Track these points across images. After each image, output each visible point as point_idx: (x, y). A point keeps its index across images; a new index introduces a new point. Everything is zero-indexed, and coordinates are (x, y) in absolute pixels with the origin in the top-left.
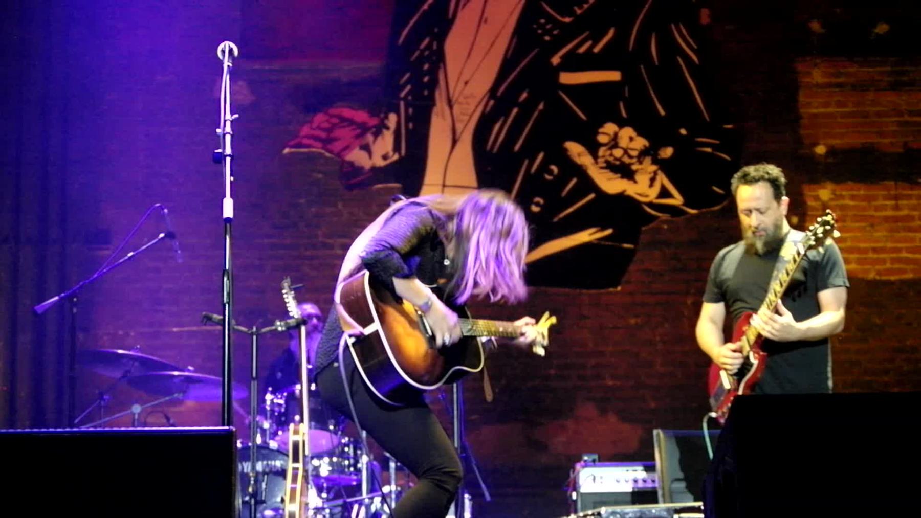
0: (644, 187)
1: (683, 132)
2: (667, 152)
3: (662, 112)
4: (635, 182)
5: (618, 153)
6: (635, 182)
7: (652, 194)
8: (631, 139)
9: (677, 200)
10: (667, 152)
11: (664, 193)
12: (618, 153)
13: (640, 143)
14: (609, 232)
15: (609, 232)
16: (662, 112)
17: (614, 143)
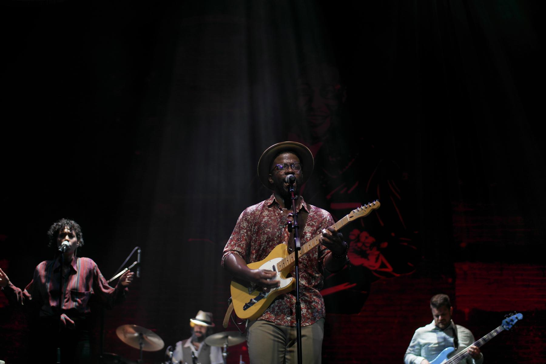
0: (372, 263)
1: (393, 234)
2: (385, 245)
3: (382, 224)
4: (368, 260)
5: (360, 245)
6: (368, 260)
7: (378, 265)
8: (366, 238)
9: (390, 269)
10: (385, 245)
11: (383, 265)
12: (360, 245)
13: (371, 240)
14: (354, 285)
15: (354, 285)
16: (382, 224)
17: (358, 239)
